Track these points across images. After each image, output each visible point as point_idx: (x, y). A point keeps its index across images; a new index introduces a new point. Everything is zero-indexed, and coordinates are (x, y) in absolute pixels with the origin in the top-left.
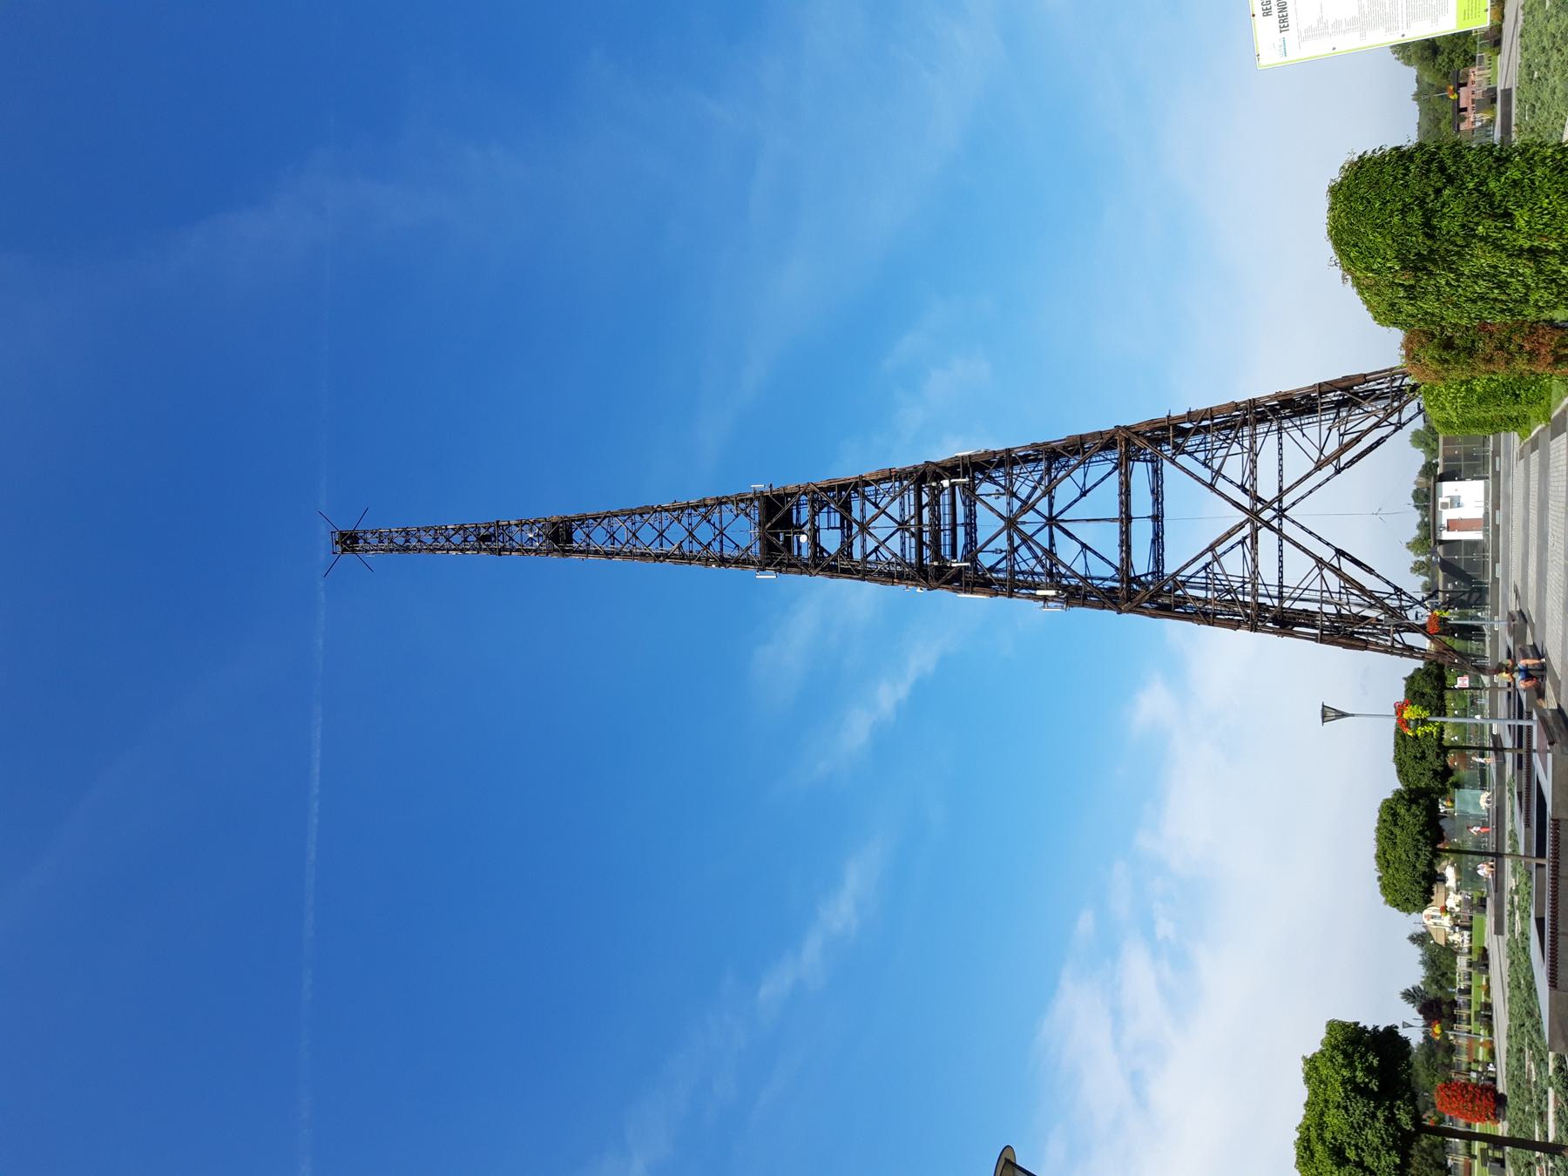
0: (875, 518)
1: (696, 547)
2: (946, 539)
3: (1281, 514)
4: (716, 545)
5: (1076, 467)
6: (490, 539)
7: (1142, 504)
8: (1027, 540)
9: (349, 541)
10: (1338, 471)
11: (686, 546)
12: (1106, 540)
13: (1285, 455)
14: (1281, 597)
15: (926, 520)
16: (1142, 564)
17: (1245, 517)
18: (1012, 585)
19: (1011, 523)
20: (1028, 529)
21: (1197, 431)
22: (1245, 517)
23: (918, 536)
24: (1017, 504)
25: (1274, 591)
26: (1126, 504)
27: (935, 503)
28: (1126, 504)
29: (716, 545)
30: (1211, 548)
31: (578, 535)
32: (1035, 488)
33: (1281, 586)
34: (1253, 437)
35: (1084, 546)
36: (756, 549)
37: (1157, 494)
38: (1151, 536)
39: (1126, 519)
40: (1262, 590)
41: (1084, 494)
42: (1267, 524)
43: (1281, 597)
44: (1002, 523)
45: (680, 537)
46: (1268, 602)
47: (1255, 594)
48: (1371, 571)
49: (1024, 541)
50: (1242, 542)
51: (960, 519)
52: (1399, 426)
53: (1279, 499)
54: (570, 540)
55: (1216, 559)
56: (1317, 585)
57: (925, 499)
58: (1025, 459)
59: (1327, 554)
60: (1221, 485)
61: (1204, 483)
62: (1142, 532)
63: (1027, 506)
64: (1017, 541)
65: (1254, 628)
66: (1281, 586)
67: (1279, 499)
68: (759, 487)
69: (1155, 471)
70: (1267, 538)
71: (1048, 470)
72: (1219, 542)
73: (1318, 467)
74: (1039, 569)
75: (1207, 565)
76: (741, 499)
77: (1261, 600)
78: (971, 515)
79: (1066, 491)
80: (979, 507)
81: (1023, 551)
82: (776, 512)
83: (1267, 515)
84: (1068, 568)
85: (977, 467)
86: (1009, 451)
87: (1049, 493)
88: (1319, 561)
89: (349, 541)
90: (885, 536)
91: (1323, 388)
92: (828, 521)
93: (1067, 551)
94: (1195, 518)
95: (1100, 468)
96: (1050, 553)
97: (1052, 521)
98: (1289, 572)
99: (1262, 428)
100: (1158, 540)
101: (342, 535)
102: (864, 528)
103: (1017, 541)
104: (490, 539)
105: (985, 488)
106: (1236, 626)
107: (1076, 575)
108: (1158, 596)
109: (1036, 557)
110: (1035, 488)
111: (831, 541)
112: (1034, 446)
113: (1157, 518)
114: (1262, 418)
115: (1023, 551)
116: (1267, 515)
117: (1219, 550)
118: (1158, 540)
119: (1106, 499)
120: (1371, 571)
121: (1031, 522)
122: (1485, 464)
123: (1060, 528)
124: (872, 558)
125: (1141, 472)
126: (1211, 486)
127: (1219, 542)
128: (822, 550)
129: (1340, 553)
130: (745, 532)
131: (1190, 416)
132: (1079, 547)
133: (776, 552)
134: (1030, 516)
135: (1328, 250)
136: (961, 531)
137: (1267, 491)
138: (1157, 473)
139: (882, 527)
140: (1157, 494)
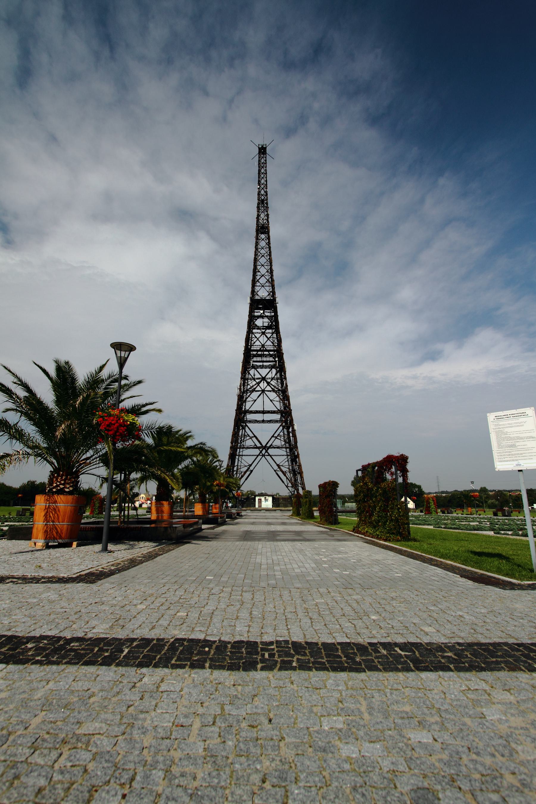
0: (266, 336)
1: (258, 277)
2: (259, 359)
3: (263, 455)
5: (279, 397)
7: (267, 417)
8: (258, 384)
9: (262, 151)
10: (275, 471)
11: (258, 274)
12: (257, 406)
13: (281, 456)
14: (239, 455)
15: (265, 353)
16: (249, 417)
17: (264, 445)
18: (244, 379)
19: (264, 379)
20: (261, 384)
21: (288, 433)
22: (264, 445)
23: (260, 350)
24: (269, 380)
25: (241, 454)
26: (268, 412)
27: (271, 356)
28: (268, 412)
30: (255, 436)
31: (263, 236)
32: (274, 386)
33: (242, 455)
34: (286, 448)
35: (255, 400)
36: (257, 297)
37: (270, 421)
38: (258, 419)
39: (263, 412)
40: (241, 450)
41: (271, 401)
42: (261, 452)
43: (239, 455)
44: (264, 376)
46: (238, 452)
47: (240, 448)
48: (246, 479)
49: (257, 383)
50: (255, 445)
51: (265, 364)
52: (287, 487)
53: (269, 455)
54: (262, 233)
55: (251, 438)
56: (242, 465)
57: (271, 353)
58: (282, 383)
59: (251, 468)
60: (273, 439)
62: (259, 417)
63: (268, 383)
64: (258, 381)
65: (231, 448)
66: (242, 455)
67: (269, 455)
69: (277, 421)
70: (257, 452)
71: (279, 390)
72: (257, 438)
73: (278, 465)
74: (249, 387)
75: (249, 436)
76: (273, 292)
77: (238, 450)
78: (266, 367)
79: (273, 395)
80: (268, 370)
81: (254, 383)
82: (270, 304)
83: (264, 451)
84: (249, 396)
85: (281, 369)
86: (285, 378)
87: (273, 390)
88: (250, 465)
89: (262, 151)
90: (261, 340)
91: (300, 466)
92: (266, 322)
93: (255, 395)
95: (279, 405)
96: (254, 390)
97: (263, 391)
98: (247, 457)
99: (288, 450)
100: (256, 421)
101: (266, 148)
102: (263, 333)
103: (258, 381)
105: (274, 371)
106: (232, 443)
107: (247, 398)
109: (253, 386)
110: (274, 386)
111: (259, 322)
112: (287, 386)
113: (263, 421)
114: (291, 450)
115: (254, 383)
116: (264, 451)
117: (254, 439)
118: (256, 421)
119: (269, 407)
120: (246, 479)
121: (263, 385)
122: (276, 507)
124: (253, 336)
125: (277, 417)
126: (273, 436)
127: (257, 438)
128: (256, 320)
129: (252, 471)
130: (263, 293)
131: (294, 431)
133: (256, 304)
134: (266, 384)
135: (385, 456)
136: (261, 364)
137: (271, 451)
138: (276, 421)
139: (263, 339)
140: (270, 421)
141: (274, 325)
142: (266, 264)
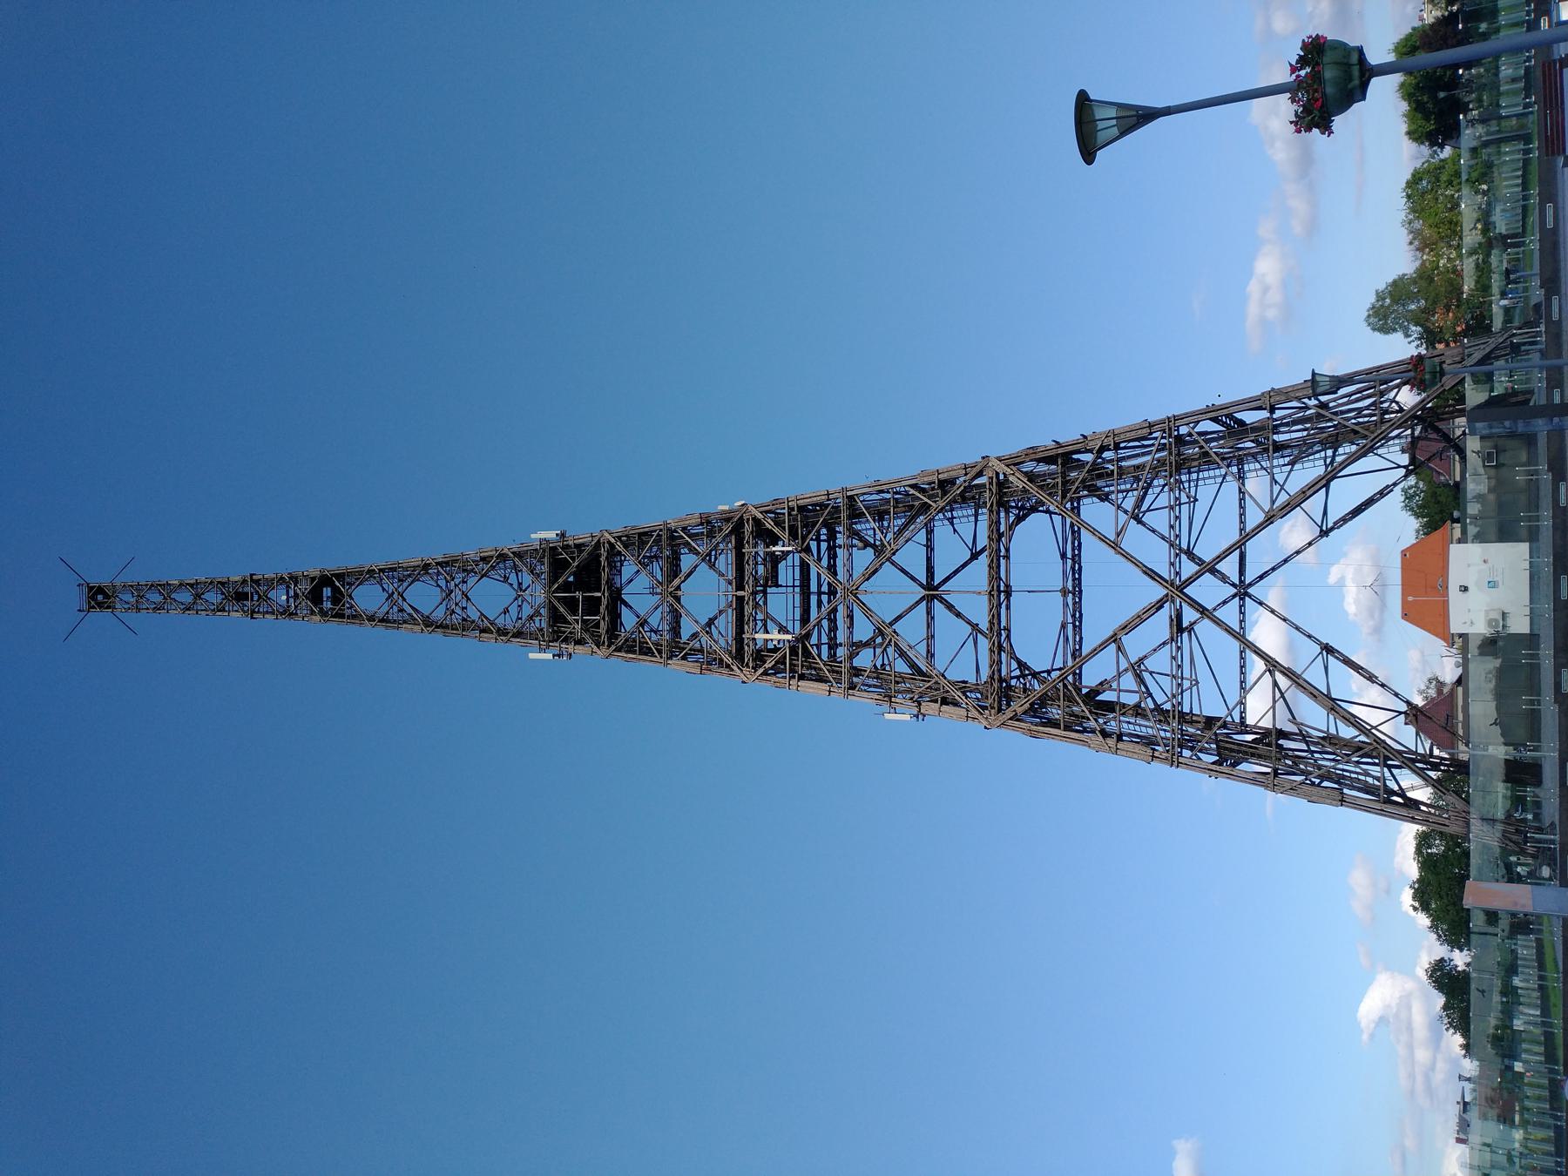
3: (1243, 591)
4: (513, 610)
6: (244, 595)
9: (99, 597)
10: (1324, 533)
13: (1217, 507)
22: (1159, 592)
29: (513, 610)
30: (1114, 638)
35: (975, 627)
39: (1000, 592)
41: (975, 556)
45: (426, 593)
48: (1371, 678)
61: (1103, 539)
68: (551, 535)
72: (1128, 627)
83: (1207, 591)
89: (99, 597)
94: (1096, 587)
104: (244, 595)
108: (1064, 705)
113: (1074, 590)
117: (1136, 643)
123: (950, 607)
126: (1115, 546)
127: (1128, 627)
129: (1328, 649)
132: (969, 629)
141: (665, 547)
142: (442, 583)
